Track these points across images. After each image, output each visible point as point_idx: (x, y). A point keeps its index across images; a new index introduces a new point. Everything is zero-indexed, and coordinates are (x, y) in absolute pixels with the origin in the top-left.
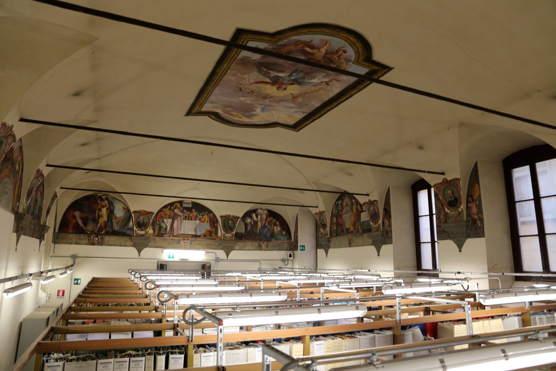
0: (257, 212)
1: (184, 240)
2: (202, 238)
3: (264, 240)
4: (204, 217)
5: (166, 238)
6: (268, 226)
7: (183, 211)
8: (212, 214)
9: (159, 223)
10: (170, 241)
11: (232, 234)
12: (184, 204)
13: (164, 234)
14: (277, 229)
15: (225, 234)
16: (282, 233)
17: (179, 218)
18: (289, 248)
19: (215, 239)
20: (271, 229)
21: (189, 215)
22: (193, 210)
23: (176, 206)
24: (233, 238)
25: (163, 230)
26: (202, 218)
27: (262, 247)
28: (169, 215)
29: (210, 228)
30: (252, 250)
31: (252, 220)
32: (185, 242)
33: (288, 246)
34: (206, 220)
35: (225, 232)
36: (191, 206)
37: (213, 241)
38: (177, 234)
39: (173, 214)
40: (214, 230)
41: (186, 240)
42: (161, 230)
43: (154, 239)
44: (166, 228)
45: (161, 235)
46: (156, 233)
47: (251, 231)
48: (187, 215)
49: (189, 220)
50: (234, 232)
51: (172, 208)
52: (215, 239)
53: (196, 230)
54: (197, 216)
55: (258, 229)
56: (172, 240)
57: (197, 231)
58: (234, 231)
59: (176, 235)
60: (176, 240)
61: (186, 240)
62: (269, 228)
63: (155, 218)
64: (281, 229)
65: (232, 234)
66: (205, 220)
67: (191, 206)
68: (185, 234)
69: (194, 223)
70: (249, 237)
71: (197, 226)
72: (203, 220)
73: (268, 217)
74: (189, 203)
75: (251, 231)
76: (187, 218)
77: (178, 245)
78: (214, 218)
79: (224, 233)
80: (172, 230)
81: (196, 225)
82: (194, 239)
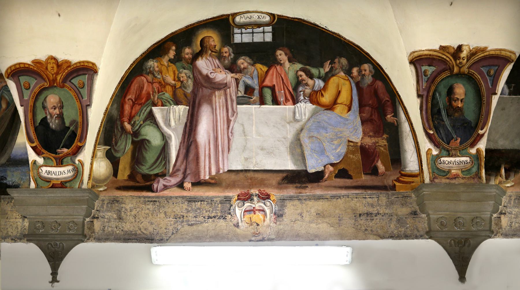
1: (246, 198)
2: (328, 187)
4: (334, 81)
5: (167, 193)
7: (234, 61)
8: (366, 66)
9: (133, 126)
10: (185, 206)
11: (470, 155)
12: (236, 30)
13: (157, 175)
15: (438, 157)
17: (218, 98)
19: (393, 188)
21: (264, 81)
22: (281, 55)
23: (202, 41)
24: (478, 175)
25: (150, 157)
26: (325, 88)
28: (174, 87)
29: (365, 133)
32: (253, 211)
34: (344, 97)
35: (437, 145)
36: (269, 38)
37: (384, 197)
38: (214, 173)
39: (190, 83)
40: (382, 142)
41: (255, 199)
42: (144, 158)
43: (115, 201)
44: (165, 149)
45: (142, 184)
46: (124, 173)
48: (256, 81)
49: (262, 102)
50: (482, 145)
51: (187, 51)
52: (393, 188)
53: (301, 145)
54: (299, 83)
56: (191, 200)
57: (307, 153)
58: (483, 135)
59: (212, 178)
60: (211, 201)
61: (255, 199)
63: (115, 106)
65: (470, 155)
66: (339, 101)
67: (269, 38)
68: (249, 171)
69: (289, 115)
71: (302, 130)
72: (327, 99)
74: (259, 25)
76: (256, 97)
77: (222, 222)
78: (379, 84)
79: (435, 152)
80: (191, 156)
81: (298, 126)
82: (291, 191)
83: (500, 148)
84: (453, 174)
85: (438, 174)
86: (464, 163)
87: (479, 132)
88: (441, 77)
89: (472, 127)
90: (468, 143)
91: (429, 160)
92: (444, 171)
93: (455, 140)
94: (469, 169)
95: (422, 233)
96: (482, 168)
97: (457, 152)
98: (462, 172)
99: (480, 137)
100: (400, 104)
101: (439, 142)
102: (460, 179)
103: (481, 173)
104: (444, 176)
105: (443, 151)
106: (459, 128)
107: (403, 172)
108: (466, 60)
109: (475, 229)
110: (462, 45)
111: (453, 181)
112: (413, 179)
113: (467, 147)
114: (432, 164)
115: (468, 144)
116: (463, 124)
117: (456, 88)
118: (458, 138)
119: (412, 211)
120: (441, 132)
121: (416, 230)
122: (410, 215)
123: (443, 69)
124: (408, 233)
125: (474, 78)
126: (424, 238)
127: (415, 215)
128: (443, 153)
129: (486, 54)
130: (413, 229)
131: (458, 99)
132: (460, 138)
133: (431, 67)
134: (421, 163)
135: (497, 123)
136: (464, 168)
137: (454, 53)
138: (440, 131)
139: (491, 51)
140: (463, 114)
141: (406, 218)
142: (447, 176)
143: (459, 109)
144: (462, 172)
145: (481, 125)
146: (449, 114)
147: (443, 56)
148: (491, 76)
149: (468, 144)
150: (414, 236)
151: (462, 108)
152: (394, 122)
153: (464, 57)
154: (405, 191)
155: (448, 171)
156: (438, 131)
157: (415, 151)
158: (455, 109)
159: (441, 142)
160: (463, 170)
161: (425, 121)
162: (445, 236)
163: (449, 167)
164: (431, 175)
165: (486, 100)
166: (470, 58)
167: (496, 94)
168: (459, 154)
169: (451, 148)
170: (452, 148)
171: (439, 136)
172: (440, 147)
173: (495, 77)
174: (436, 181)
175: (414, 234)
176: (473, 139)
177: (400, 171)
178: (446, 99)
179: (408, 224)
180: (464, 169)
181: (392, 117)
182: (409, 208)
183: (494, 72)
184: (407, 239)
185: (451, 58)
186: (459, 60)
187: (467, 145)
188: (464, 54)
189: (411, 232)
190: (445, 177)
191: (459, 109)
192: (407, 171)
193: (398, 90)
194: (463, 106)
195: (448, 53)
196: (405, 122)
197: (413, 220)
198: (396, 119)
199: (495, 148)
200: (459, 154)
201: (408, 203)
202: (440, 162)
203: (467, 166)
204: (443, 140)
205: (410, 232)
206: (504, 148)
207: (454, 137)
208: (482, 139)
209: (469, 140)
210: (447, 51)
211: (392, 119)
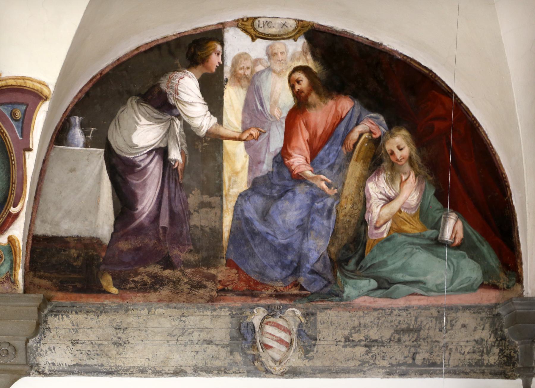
0: (215, 60)
3: (279, 296)
6: (309, 173)
14: (389, 200)
16: (437, 226)
18: (492, 359)
20: (338, 196)
27: (267, 347)
30: (178, 372)
31: (169, 132)
33: (485, 334)
47: (164, 221)
55: (229, 206)
62: (321, 195)
64: (432, 192)
70: (155, 269)
73: (313, 98)
75: (164, 221)
87: (10, 210)
96: (17, 266)
135: (61, 192)
145: (12, 198)
148: (18, 120)
199: (55, 235)
206: (69, 235)
208: (16, 221)
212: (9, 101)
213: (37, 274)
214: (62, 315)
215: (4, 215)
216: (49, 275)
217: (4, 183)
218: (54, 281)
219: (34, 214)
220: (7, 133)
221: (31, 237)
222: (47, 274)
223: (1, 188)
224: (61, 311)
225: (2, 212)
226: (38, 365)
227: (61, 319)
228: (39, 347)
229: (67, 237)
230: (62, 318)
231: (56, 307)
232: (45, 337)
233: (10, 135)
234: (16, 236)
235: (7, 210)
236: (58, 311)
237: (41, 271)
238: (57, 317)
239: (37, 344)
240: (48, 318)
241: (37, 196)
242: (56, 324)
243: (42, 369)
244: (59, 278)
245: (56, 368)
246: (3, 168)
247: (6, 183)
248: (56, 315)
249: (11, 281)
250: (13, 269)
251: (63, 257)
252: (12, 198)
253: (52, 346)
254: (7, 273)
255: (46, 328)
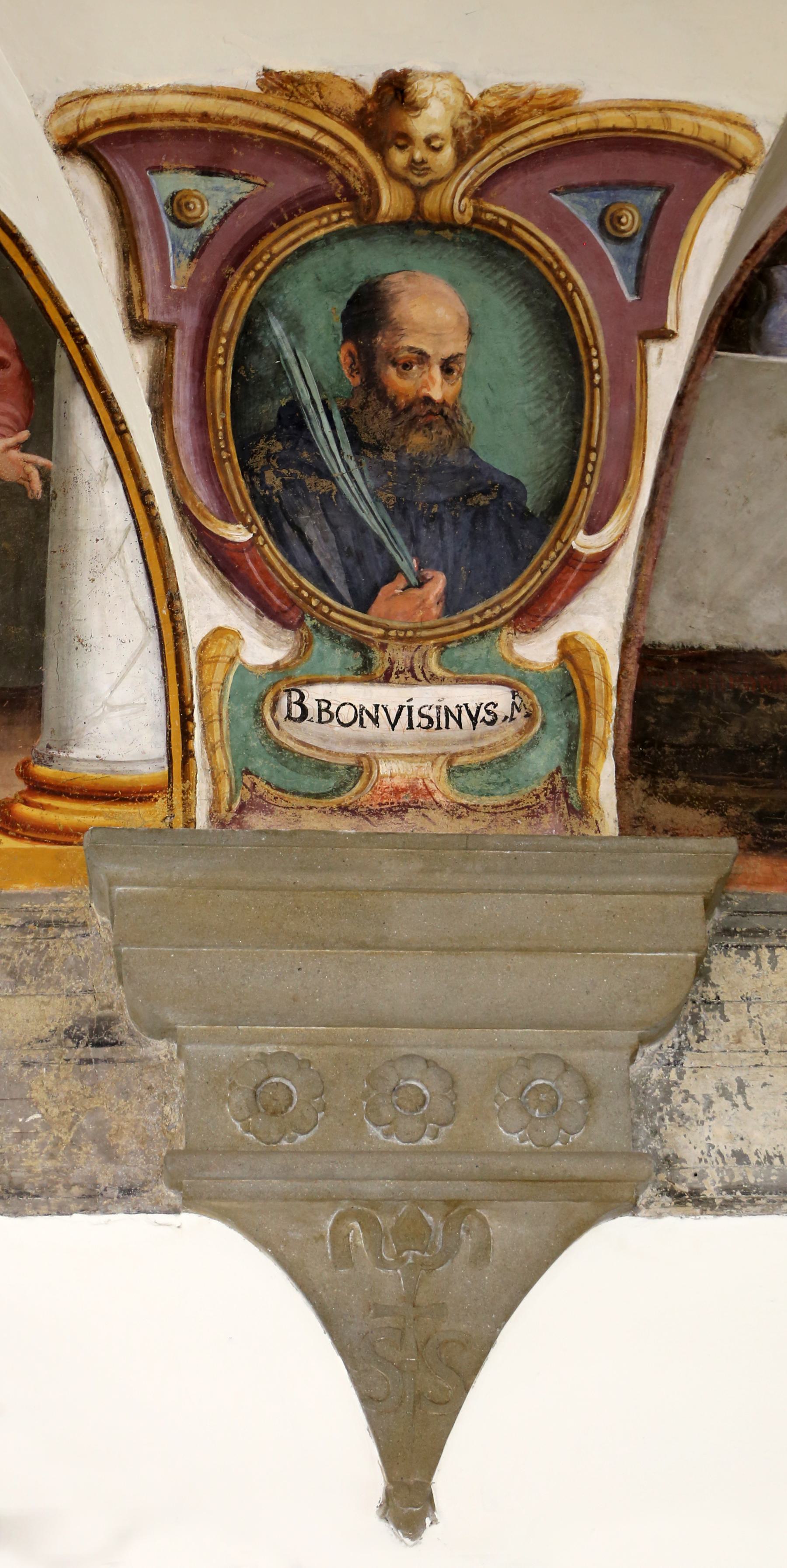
58: (600, 561)
83: (764, 643)
84: (387, 781)
85: (274, 781)
86: (474, 719)
88: (293, 236)
89: (525, 516)
90: (499, 603)
91: (215, 696)
92: (324, 768)
93: (409, 586)
94: (505, 758)
95: (134, 1170)
96: (595, 748)
97: (424, 656)
98: (454, 771)
99: (582, 570)
100: (80, 379)
101: (297, 592)
102: (431, 814)
103: (592, 779)
104: (318, 796)
105: (321, 645)
106: (437, 518)
107: (41, 771)
108: (448, 153)
109: (516, 1138)
110: (405, 74)
111: (390, 825)
112: (113, 816)
113: (497, 629)
114: (234, 722)
115: (504, 612)
116: (468, 495)
117: (404, 298)
118: (429, 574)
119: (83, 1020)
120: (311, 532)
121: (91, 1148)
122: (60, 1043)
123: (302, 197)
124: (29, 1170)
125: (518, 246)
126: (146, 1203)
127: (98, 1045)
128: (321, 655)
129: (571, 124)
130: (67, 1138)
131: (423, 357)
132: (445, 572)
133: (218, 181)
134: (186, 719)
135: (747, 500)
136: (468, 747)
137: (362, 112)
138: (301, 534)
139: (601, 109)
140: (460, 440)
141: (26, 1064)
142: (346, 798)
143: (430, 413)
144: (449, 772)
146: (365, 438)
147: (295, 126)
149: (504, 612)
150: (76, 1191)
151: (455, 408)
152: (28, 478)
153: (436, 137)
154: (47, 890)
155: (350, 768)
156: (288, 529)
157: (153, 645)
158: (407, 409)
159: (312, 595)
160: (460, 761)
161: (191, 468)
162: (287, 1185)
163: (361, 742)
164: (225, 789)
165: (611, 366)
166: (477, 144)
167: (666, 335)
168: (433, 666)
169: (381, 631)
170: (387, 629)
171: (292, 560)
172: (302, 621)
173: (653, 244)
174: (257, 821)
175: (76, 1175)
176: (536, 581)
177: (25, 764)
178: (342, 354)
179: (33, 1105)
180: (470, 753)
181: (15, 454)
182: (58, 1001)
183: (642, 219)
184: (16, 1214)
185: (351, 138)
186: (402, 148)
187: (498, 616)
188: (431, 121)
189: (49, 1164)
190: (324, 802)
191: (430, 413)
192: (75, 766)
193: (71, 306)
194: (460, 394)
195: (326, 110)
196: (103, 480)
197: (82, 1077)
198: (42, 461)
199: (727, 644)
200: (433, 666)
201: (56, 965)
202: (297, 711)
203: (494, 740)
204: (323, 580)
205: (41, 1164)
207: (403, 565)
208: (595, 583)
209: (511, 589)
210: (318, 100)
211: (13, 462)
212: (596, 178)
213: (661, 786)
214: (771, 948)
215: (546, 563)
216: (711, 788)
217: (555, 450)
218: (732, 812)
219: (646, 570)
220: (581, 283)
221: (633, 652)
222: (700, 788)
223: (543, 467)
224: (766, 933)
225: (542, 552)
226: (670, 1161)
227: (766, 965)
228: (676, 1083)
229: (777, 653)
230: (773, 961)
231: (744, 913)
232: (701, 1039)
233: (590, 288)
234: (594, 635)
235: (559, 545)
236: (754, 932)
237: (675, 777)
238: (752, 954)
239: (667, 1072)
240: (714, 958)
241: (656, 510)
242: (748, 986)
243: (691, 1179)
244: (752, 802)
245: (751, 1175)
246: (557, 396)
247: (561, 450)
248: (744, 949)
249: (570, 807)
250: (580, 758)
251: (765, 726)
252: (582, 500)
253: (731, 1077)
254: (552, 776)
255: (705, 1002)
